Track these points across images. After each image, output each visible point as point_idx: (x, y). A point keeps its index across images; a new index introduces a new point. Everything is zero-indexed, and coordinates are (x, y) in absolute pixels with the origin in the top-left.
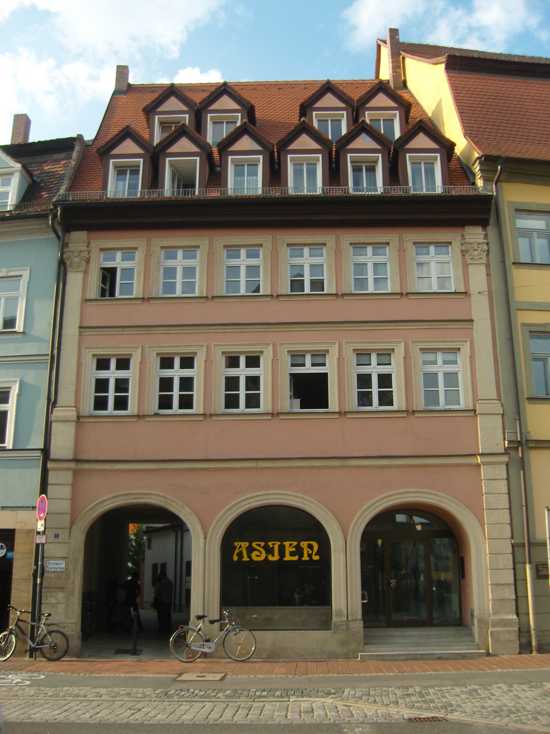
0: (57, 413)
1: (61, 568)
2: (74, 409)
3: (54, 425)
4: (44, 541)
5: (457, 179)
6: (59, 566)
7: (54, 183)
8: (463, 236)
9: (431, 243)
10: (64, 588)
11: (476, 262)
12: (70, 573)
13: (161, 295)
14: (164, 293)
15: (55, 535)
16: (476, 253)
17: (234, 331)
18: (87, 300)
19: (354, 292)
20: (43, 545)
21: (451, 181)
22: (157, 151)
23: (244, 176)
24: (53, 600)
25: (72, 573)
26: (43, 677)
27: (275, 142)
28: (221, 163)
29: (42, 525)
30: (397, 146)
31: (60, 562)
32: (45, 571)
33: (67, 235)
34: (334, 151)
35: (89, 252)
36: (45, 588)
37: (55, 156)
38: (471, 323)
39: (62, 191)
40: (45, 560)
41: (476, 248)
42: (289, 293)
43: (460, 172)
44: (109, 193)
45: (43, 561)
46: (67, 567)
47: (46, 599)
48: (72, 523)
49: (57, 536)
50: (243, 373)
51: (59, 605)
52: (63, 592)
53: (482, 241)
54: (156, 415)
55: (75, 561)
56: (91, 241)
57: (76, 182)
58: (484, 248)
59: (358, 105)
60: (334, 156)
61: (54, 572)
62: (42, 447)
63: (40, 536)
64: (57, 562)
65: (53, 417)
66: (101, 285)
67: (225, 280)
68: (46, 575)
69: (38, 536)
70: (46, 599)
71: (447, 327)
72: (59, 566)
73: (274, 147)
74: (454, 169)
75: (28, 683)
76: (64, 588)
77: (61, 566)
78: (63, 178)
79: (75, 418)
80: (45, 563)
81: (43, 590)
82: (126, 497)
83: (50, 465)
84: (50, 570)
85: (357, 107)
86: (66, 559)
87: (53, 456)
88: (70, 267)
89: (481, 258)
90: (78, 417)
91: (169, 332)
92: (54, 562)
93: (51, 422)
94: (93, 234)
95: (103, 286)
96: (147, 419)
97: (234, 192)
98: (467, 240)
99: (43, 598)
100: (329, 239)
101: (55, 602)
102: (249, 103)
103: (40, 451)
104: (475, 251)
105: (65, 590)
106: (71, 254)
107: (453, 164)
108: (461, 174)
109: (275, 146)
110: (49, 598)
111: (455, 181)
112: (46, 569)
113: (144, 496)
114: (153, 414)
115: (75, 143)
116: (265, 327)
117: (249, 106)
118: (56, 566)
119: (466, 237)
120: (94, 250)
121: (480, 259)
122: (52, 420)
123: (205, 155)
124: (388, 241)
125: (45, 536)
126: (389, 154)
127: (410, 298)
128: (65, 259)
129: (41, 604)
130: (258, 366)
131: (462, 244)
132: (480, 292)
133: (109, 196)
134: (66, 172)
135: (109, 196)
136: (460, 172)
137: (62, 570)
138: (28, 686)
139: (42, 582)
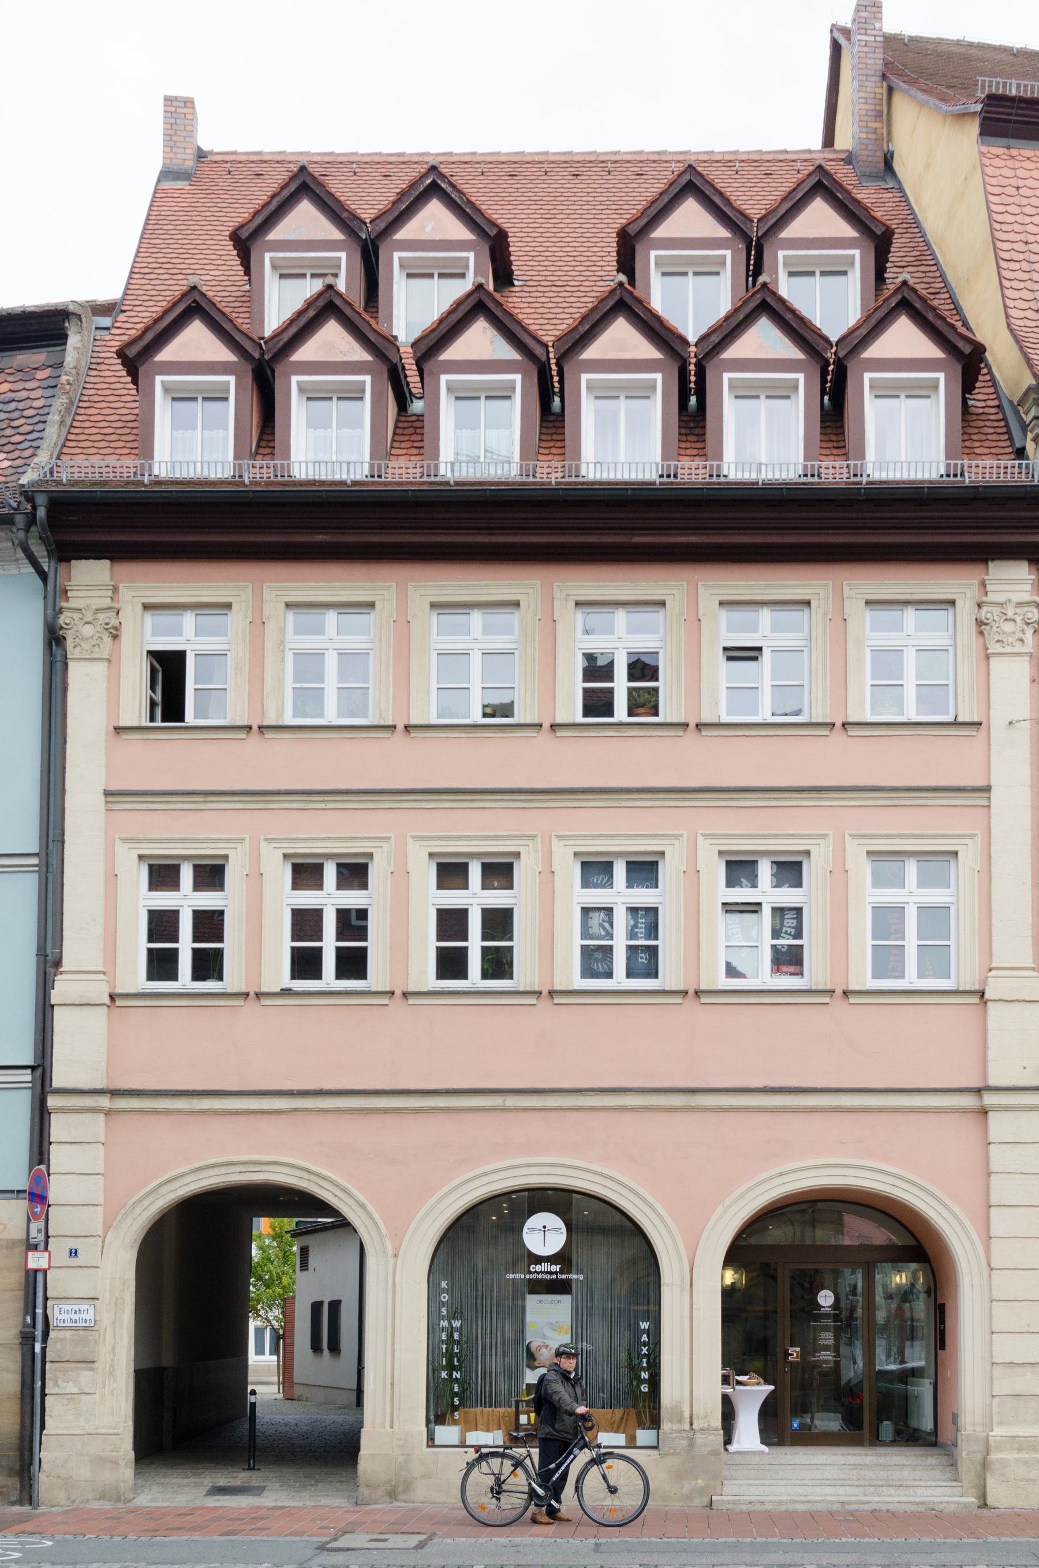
0: (61, 990)
1: (86, 1321)
2: (102, 977)
3: (58, 1014)
4: (46, 1266)
5: (984, 437)
6: (81, 1316)
7: (21, 430)
8: (983, 584)
9: (907, 603)
10: (94, 1362)
11: (1008, 649)
12: (105, 1330)
13: (289, 720)
14: (295, 716)
15: (71, 1253)
16: (1008, 627)
17: (454, 805)
18: (118, 730)
19: (725, 719)
20: (45, 1272)
21: (967, 444)
22: (266, 357)
23: (479, 428)
24: (70, 1388)
25: (109, 1332)
26: (49, 1543)
27: (553, 338)
28: (423, 388)
29: (39, 1231)
30: (841, 354)
31: (83, 1307)
32: (51, 1327)
33: (63, 567)
34: (693, 373)
35: (118, 613)
36: (52, 1362)
37: (19, 357)
38: (986, 795)
39: (43, 458)
40: (49, 1303)
41: (1010, 615)
42: (580, 719)
43: (992, 417)
44: (156, 466)
45: (45, 1307)
46: (98, 1318)
47: (56, 1385)
48: (107, 1226)
49: (74, 1253)
50: (474, 901)
51: (83, 1397)
52: (92, 1369)
53: (1026, 597)
54: (286, 992)
55: (116, 1304)
56: (121, 585)
57: (77, 431)
58: (1030, 615)
59: (760, 234)
60: (692, 385)
61: (70, 1329)
62: (32, 1063)
63: (37, 1254)
64: (76, 1307)
65: (55, 997)
66: (149, 692)
67: (434, 685)
68: (52, 1334)
69: (30, 1254)
70: (56, 1385)
71: (930, 802)
72: (81, 1316)
73: (548, 352)
74: (981, 411)
75: (17, 1555)
76: (94, 1362)
77: (85, 1316)
78: (43, 418)
79: (107, 1000)
80: (49, 1311)
81: (48, 1366)
82: (223, 1170)
83: (52, 1102)
84: (62, 1324)
85: (758, 239)
86: (96, 1302)
87: (57, 1082)
88: (75, 647)
89: (1022, 640)
90: (112, 997)
91: (311, 806)
92: (69, 1307)
93: (53, 1006)
94: (128, 569)
95: (153, 694)
96: (265, 1002)
97: (452, 471)
98: (992, 597)
99: (49, 1384)
100: (673, 592)
101: (76, 1391)
102: (493, 224)
103: (29, 1071)
104: (1007, 622)
105: (96, 1365)
106: (76, 616)
107: (980, 397)
108: (996, 424)
109: (551, 349)
110: (60, 1383)
111: (977, 444)
112: (53, 1323)
113: (264, 1168)
114: (278, 990)
115: (67, 324)
116: (524, 797)
117: (493, 232)
118: (74, 1317)
119: (989, 588)
120: (129, 607)
121: (1019, 643)
122: (52, 1002)
123: (384, 370)
124: (807, 597)
125: (46, 1254)
126: (824, 382)
127: (850, 733)
128: (62, 628)
129: (44, 1395)
130: (508, 884)
131: (979, 606)
132: (1010, 723)
133: (156, 472)
134: (48, 402)
135: (156, 472)
136: (992, 417)
137: (87, 1325)
138: (16, 1561)
139: (44, 1350)
